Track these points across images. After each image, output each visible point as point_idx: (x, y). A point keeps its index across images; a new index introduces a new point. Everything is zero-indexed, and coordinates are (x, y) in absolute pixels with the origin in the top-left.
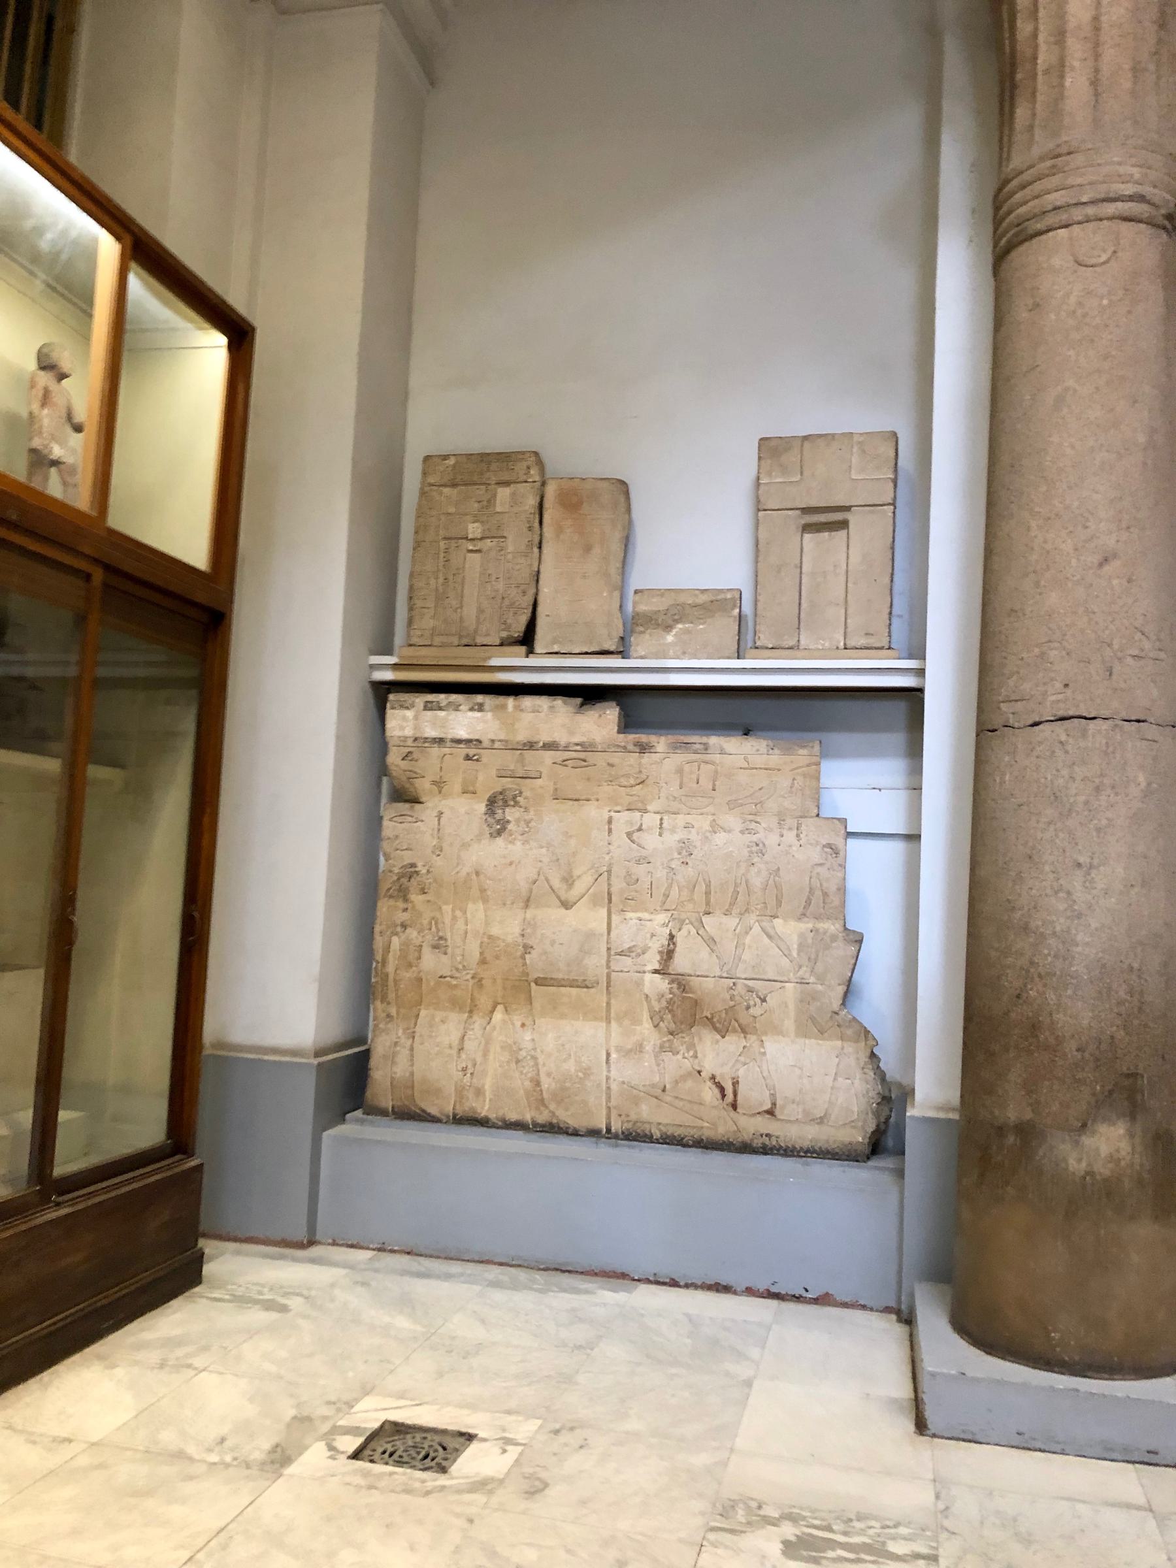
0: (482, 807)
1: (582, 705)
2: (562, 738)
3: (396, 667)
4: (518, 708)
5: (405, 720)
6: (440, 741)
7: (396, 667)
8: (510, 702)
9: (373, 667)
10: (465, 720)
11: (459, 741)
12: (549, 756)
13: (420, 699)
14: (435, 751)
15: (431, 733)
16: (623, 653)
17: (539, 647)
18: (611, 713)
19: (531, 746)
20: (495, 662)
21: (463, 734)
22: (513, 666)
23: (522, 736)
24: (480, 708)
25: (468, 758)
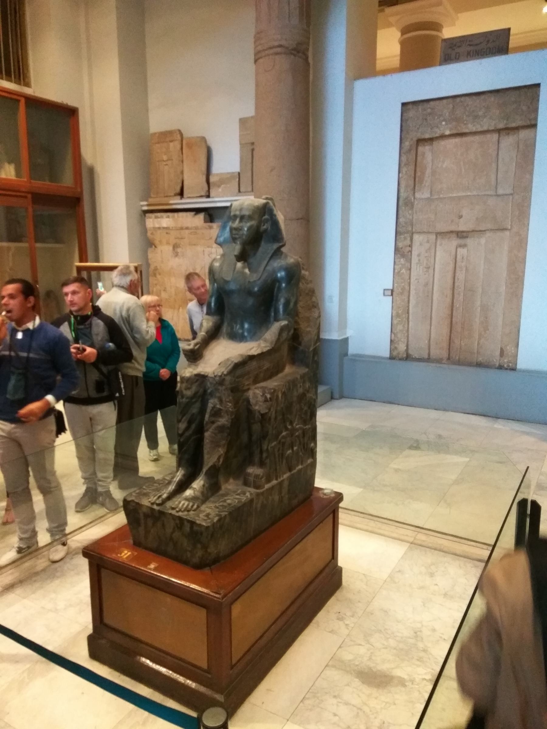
0: (171, 248)
1: (195, 214)
2: (189, 225)
3: (148, 205)
4: (178, 217)
5: (151, 222)
6: (159, 228)
7: (148, 205)
8: (176, 214)
9: (142, 206)
10: (166, 221)
11: (164, 228)
12: (187, 232)
13: (153, 215)
14: (159, 232)
15: (157, 226)
16: (208, 196)
17: (185, 196)
18: (201, 216)
19: (182, 228)
20: (171, 202)
21: (165, 225)
22: (176, 202)
23: (179, 225)
24: (168, 217)
25: (167, 233)
